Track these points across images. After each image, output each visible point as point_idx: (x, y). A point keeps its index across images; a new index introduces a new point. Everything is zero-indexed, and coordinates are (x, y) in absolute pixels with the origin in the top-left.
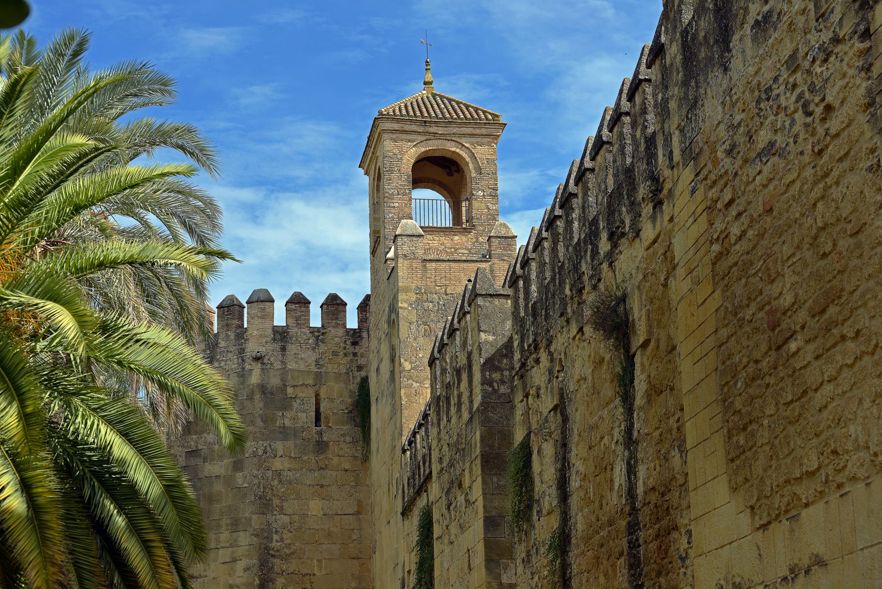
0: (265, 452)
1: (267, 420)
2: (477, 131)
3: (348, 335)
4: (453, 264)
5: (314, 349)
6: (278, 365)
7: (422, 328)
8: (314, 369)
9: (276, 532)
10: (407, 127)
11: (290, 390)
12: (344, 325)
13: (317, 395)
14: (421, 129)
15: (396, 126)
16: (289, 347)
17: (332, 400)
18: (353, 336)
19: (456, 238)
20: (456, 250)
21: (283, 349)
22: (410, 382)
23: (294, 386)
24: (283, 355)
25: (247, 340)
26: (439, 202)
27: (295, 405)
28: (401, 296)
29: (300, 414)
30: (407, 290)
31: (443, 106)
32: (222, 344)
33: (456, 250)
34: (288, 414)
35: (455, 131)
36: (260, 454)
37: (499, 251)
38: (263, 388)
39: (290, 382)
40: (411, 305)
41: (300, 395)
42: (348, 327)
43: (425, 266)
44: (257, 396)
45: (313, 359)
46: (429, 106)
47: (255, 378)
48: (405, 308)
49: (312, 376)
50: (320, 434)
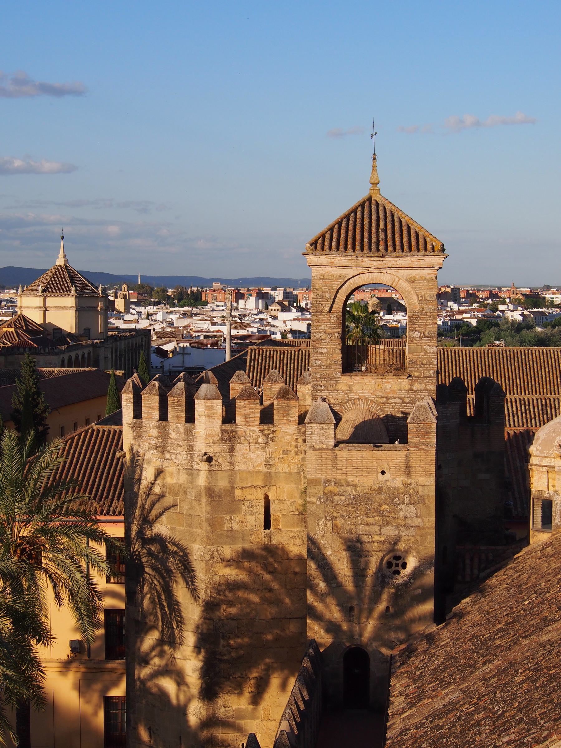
0: (212, 557)
1: (214, 524)
2: (416, 264)
5: (263, 448)
6: (225, 467)
8: (264, 469)
9: (223, 637)
11: (238, 493)
13: (267, 498)
16: (237, 447)
17: (281, 501)
20: (388, 398)
21: (232, 449)
23: (242, 488)
24: (231, 456)
25: (196, 437)
27: (243, 508)
29: (249, 517)
32: (173, 435)
33: (388, 398)
34: (237, 518)
36: (207, 559)
37: (416, 439)
38: (210, 492)
39: (238, 483)
40: (320, 498)
41: (249, 497)
44: (204, 500)
45: (263, 459)
47: (202, 480)
48: (313, 503)
49: (261, 477)
50: (269, 536)
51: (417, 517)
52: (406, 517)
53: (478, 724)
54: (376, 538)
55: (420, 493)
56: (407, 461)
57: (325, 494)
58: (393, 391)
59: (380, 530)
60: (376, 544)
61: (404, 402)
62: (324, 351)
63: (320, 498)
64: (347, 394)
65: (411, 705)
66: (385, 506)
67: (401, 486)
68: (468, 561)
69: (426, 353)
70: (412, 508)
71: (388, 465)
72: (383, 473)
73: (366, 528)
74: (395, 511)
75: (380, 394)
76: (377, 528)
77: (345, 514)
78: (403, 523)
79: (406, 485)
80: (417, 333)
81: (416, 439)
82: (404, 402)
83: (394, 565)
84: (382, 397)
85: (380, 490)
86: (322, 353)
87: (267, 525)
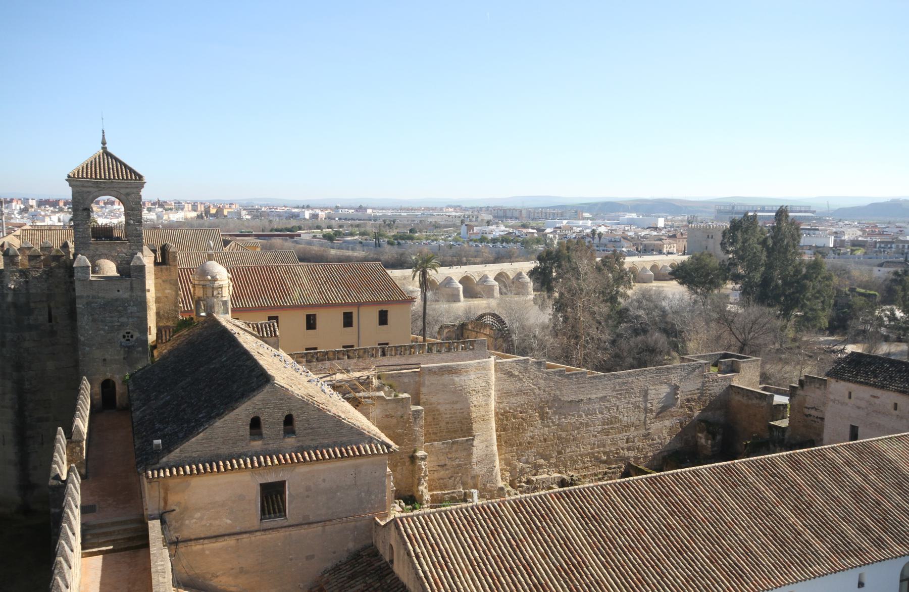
7: (90, 318)
28: (78, 301)
30: (81, 297)
53: (184, 410)
56: (131, 284)
57: (87, 303)
65: (144, 405)
74: (125, 309)
85: (117, 300)
87: (50, 321)
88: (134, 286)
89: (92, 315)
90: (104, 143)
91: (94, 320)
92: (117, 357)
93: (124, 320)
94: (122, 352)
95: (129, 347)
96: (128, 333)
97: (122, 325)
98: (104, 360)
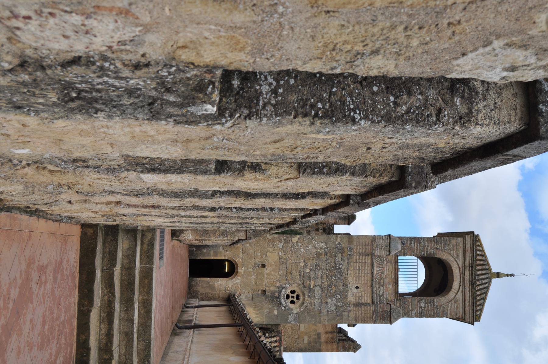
2: (467, 304)
3: (330, 225)
4: (369, 275)
7: (322, 251)
10: (468, 254)
12: (335, 223)
14: (467, 263)
15: (468, 246)
18: (329, 228)
19: (391, 286)
20: (383, 286)
22: (283, 241)
26: (416, 285)
31: (483, 282)
33: (383, 286)
35: (467, 288)
37: (380, 310)
40: (339, 244)
42: (335, 225)
43: (368, 255)
46: (483, 272)
48: (336, 240)
51: (328, 311)
52: (327, 303)
54: (313, 283)
55: (343, 313)
56: (365, 304)
57: (342, 248)
58: (387, 290)
59: (318, 285)
60: (308, 282)
61: (381, 296)
62: (413, 245)
63: (339, 244)
64: (386, 260)
66: (334, 289)
67: (348, 300)
68: (275, 339)
69: (412, 310)
70: (333, 308)
71: (363, 291)
72: (357, 288)
73: (320, 276)
74: (331, 296)
75: (386, 281)
76: (319, 284)
77: (329, 261)
78: (323, 302)
79: (348, 304)
80: (424, 305)
81: (380, 310)
82: (381, 296)
83: (293, 295)
84: (383, 282)
85: (345, 285)
86: (411, 243)
88: (363, 308)
89: (326, 254)
90: (498, 275)
91: (318, 255)
92: (266, 281)
93: (318, 292)
94: (273, 289)
95: (279, 298)
96: (298, 297)
97: (311, 290)
98: (264, 266)
